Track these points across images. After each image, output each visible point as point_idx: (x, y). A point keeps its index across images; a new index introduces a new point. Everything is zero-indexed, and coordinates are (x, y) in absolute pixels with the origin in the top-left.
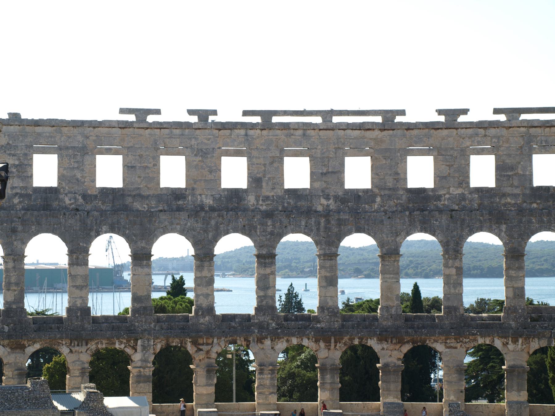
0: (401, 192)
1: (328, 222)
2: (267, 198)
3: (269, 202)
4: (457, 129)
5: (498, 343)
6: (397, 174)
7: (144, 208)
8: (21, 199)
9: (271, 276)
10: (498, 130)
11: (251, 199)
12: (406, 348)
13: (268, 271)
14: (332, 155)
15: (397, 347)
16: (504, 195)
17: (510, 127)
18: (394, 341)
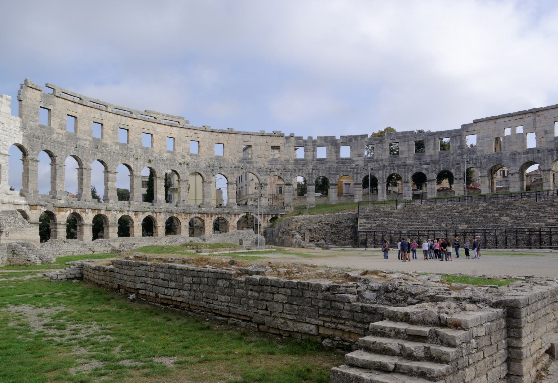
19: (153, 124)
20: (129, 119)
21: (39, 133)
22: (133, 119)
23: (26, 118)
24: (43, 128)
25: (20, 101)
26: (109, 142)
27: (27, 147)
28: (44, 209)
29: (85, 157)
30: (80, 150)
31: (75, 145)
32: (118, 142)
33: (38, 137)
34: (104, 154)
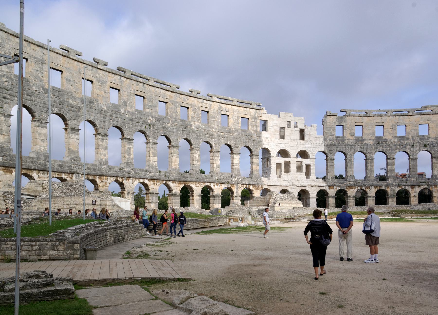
0: (178, 120)
1: (153, 128)
2: (128, 112)
3: (130, 114)
4: (197, 98)
5: (212, 185)
6: (177, 112)
7: (74, 103)
8: (7, 80)
9: (131, 149)
10: (210, 102)
11: (122, 110)
12: (182, 186)
13: (130, 146)
14: (154, 98)
15: (179, 185)
16: (212, 128)
17: (214, 102)
18: (178, 182)
19: (429, 116)
20: (406, 117)
21: (336, 142)
22: (410, 116)
23: (327, 135)
24: (338, 138)
25: (323, 125)
26: (389, 137)
27: (327, 152)
28: (338, 188)
29: (369, 151)
30: (365, 147)
31: (361, 145)
32: (397, 136)
33: (335, 145)
34: (384, 146)
